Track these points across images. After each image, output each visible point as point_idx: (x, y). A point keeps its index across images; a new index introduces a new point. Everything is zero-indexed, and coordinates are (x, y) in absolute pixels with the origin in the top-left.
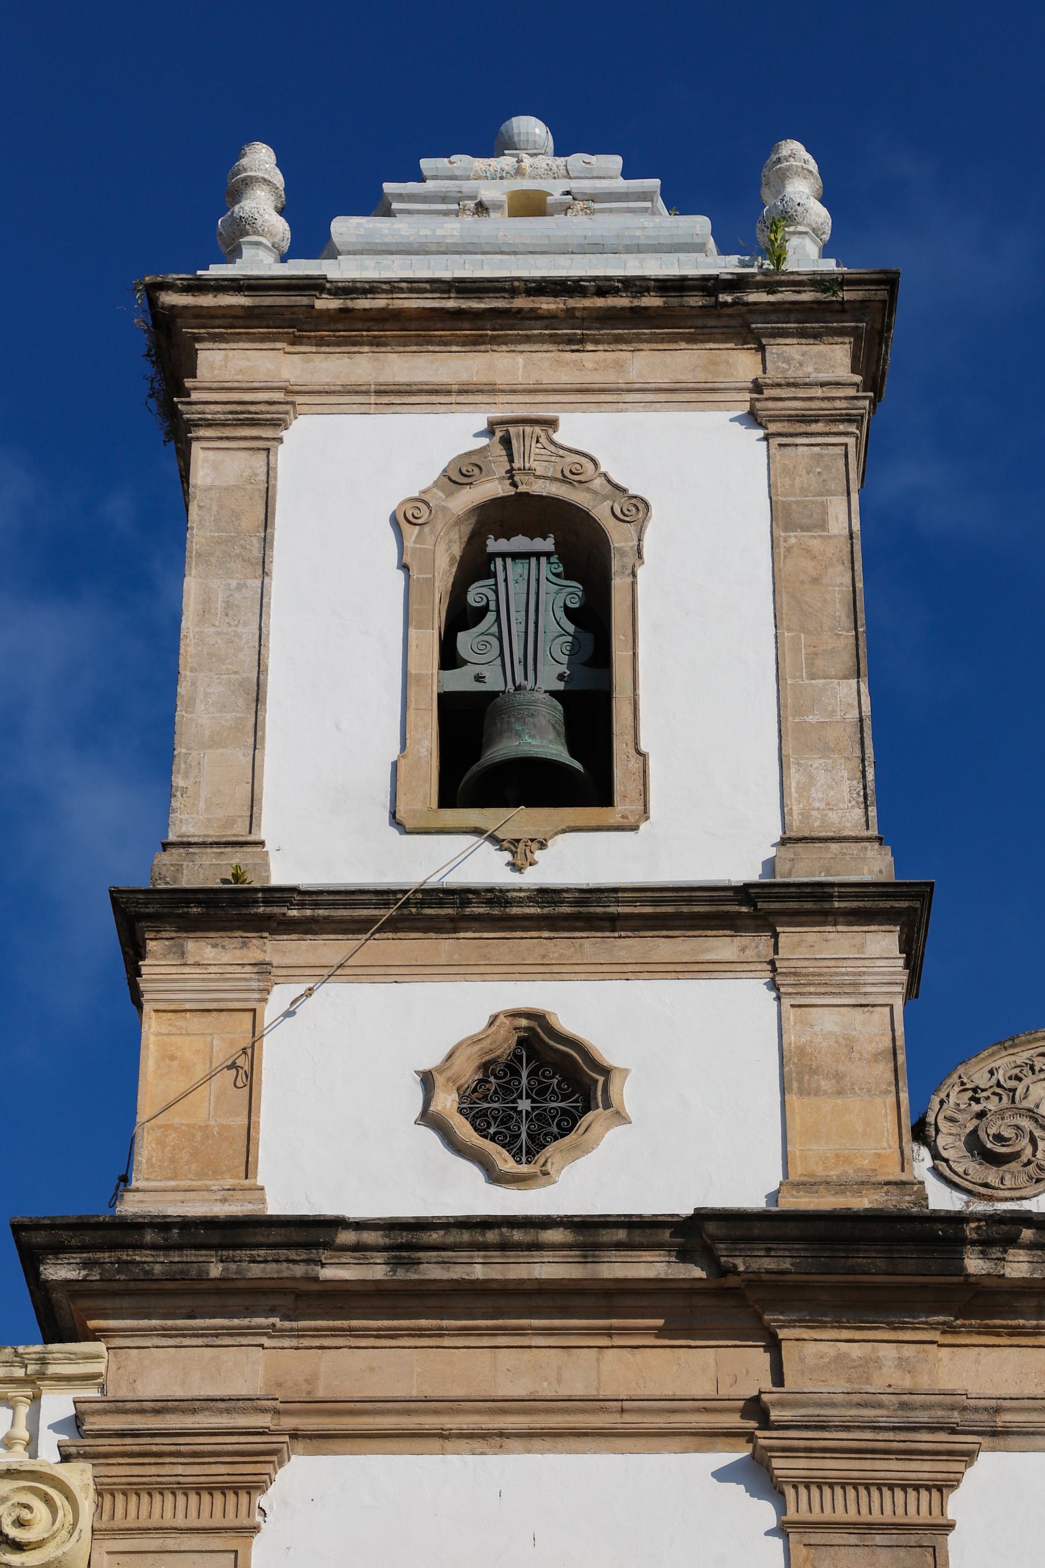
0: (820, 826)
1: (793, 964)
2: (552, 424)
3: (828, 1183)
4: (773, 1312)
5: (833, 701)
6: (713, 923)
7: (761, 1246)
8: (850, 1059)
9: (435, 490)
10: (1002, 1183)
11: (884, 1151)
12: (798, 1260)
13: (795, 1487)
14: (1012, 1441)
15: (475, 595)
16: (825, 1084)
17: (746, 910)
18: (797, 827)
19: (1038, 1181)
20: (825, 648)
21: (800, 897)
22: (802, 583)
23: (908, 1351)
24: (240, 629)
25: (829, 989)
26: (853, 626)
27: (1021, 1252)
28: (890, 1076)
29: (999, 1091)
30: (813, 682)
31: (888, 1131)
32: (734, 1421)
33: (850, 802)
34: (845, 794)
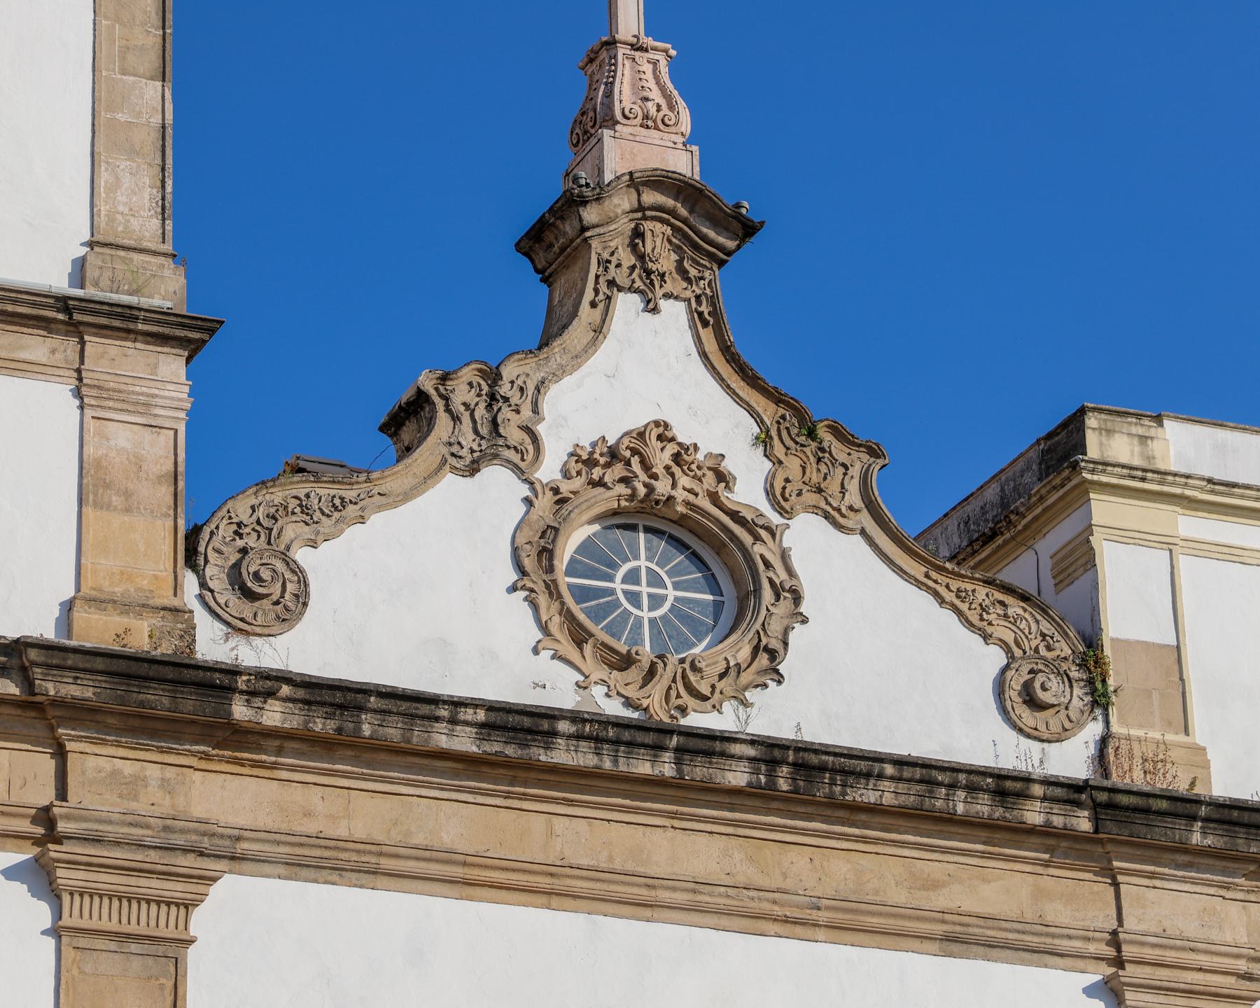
0: (123, 232)
1: (97, 376)
3: (115, 602)
4: (66, 728)
5: (140, 102)
6: (31, 323)
7: (70, 674)
8: (138, 477)
10: (255, 619)
11: (160, 573)
12: (99, 691)
13: (71, 894)
14: (247, 866)
16: (117, 500)
17: (62, 318)
18: (104, 229)
19: (284, 620)
20: (135, 43)
21: (109, 315)
23: (170, 772)
25: (125, 406)
26: (161, 24)
27: (277, 703)
28: (170, 500)
29: (258, 528)
30: (124, 77)
31: (165, 554)
32: (25, 826)
33: (150, 211)
34: (146, 201)
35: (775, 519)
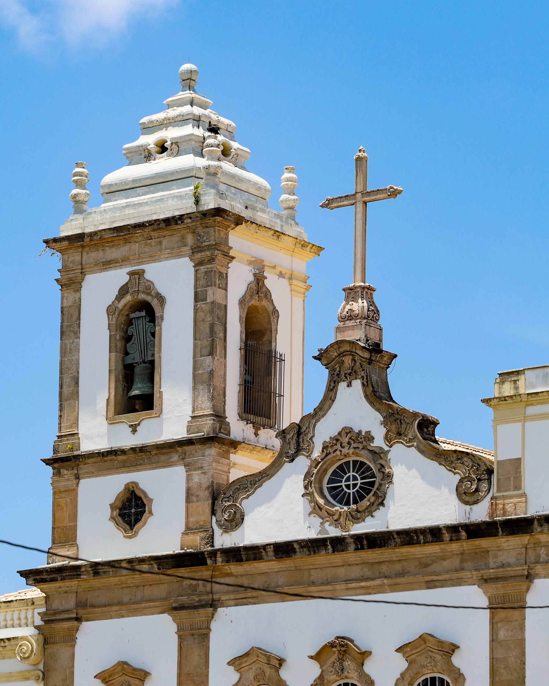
2: (143, 271)
9: (116, 301)
15: (131, 330)
16: (195, 499)
22: (200, 321)
24: (73, 358)
35: (386, 448)
